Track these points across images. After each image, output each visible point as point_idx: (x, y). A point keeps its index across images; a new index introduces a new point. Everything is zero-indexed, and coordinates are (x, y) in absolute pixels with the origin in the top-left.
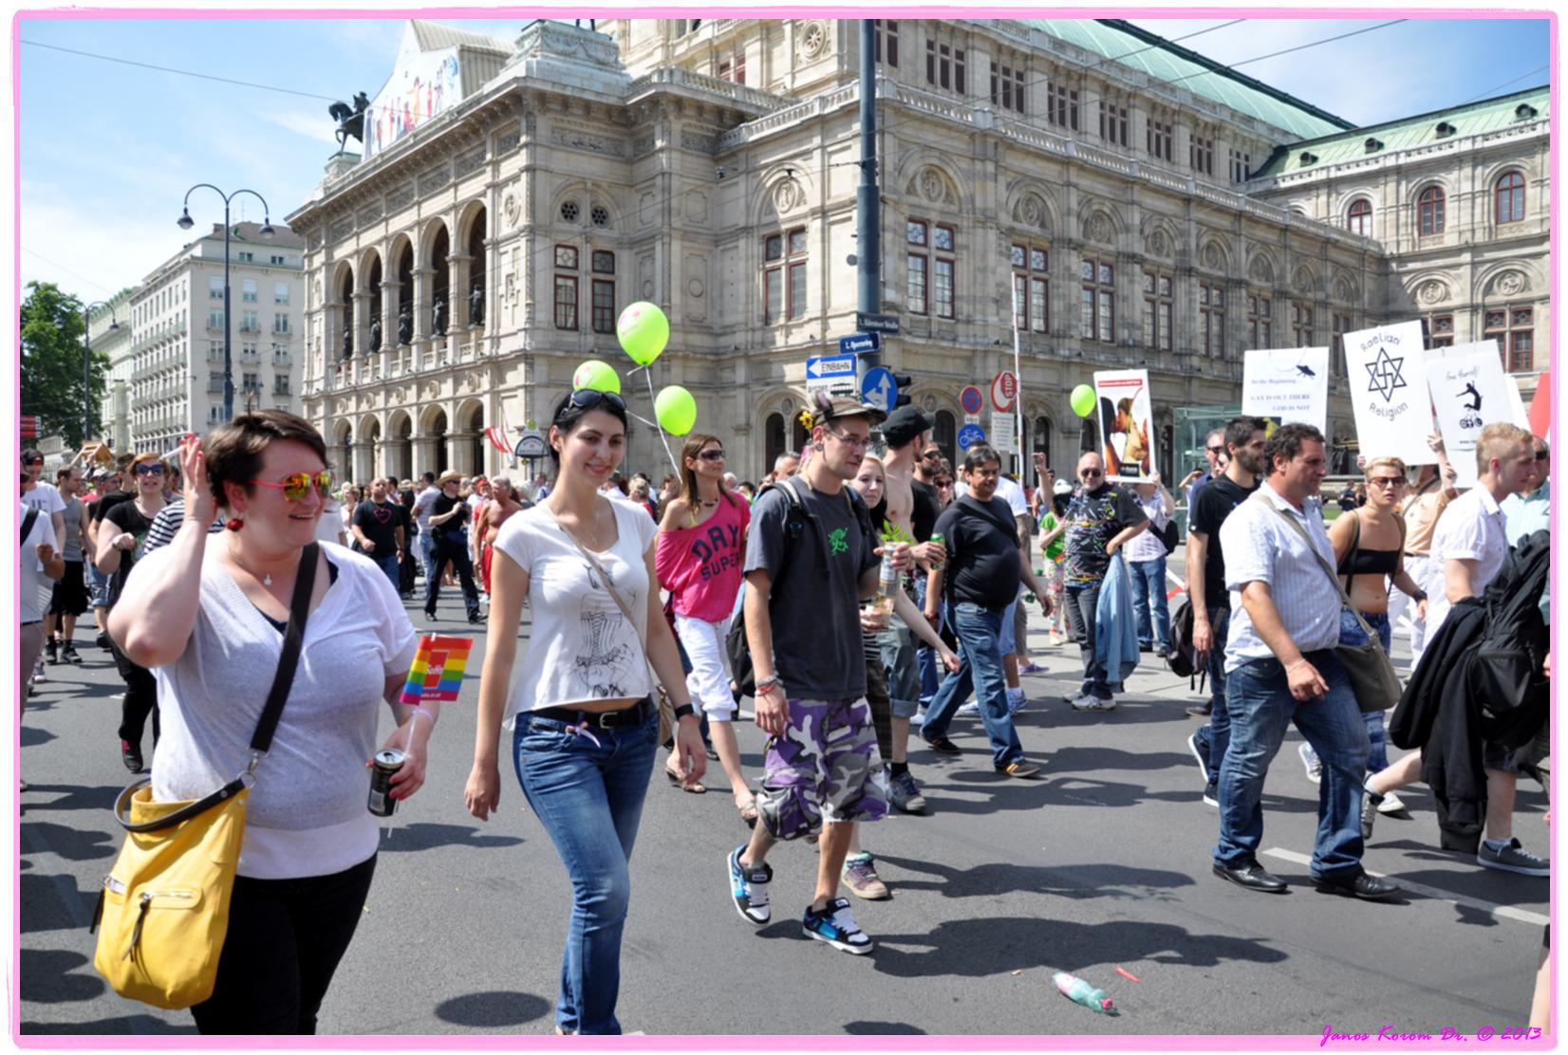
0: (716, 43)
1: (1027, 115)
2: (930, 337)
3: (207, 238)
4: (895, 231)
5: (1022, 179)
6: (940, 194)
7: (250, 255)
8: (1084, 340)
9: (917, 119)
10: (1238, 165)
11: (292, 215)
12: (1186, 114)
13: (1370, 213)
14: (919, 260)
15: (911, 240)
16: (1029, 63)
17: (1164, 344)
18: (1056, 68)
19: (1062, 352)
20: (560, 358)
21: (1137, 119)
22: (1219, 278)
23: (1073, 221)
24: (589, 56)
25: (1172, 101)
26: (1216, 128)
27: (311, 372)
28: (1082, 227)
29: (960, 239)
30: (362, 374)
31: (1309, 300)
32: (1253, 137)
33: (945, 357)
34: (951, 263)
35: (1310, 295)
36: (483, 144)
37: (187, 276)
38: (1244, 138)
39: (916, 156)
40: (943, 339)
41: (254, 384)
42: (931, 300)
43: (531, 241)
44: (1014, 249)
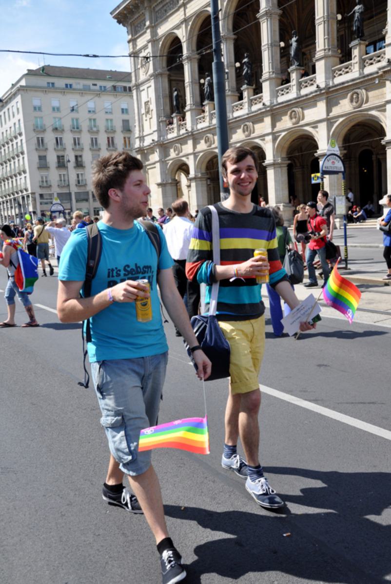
3: (27, 74)
7: (53, 84)
11: (118, 7)
27: (142, 128)
30: (195, 122)
37: (18, 98)
41: (63, 162)
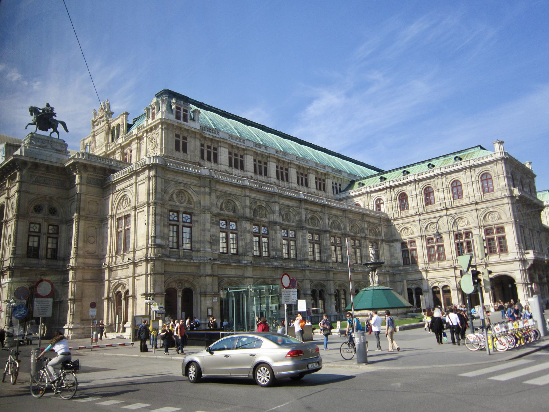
0: (122, 145)
1: (245, 171)
2: (179, 258)
4: (161, 216)
5: (225, 194)
6: (185, 201)
8: (254, 257)
9: (173, 171)
10: (336, 188)
12: (312, 170)
13: (383, 203)
14: (175, 228)
15: (171, 218)
16: (245, 152)
17: (293, 256)
18: (256, 154)
19: (244, 262)
20: (26, 270)
21: (292, 172)
22: (317, 230)
23: (248, 210)
24: (52, 148)
25: (307, 166)
26: (326, 174)
28: (252, 212)
29: (194, 218)
31: (358, 237)
32: (342, 177)
33: (187, 266)
34: (191, 228)
35: (359, 235)
38: (338, 178)
39: (174, 186)
40: (186, 259)
42: (181, 243)
43: (17, 221)
44: (221, 222)
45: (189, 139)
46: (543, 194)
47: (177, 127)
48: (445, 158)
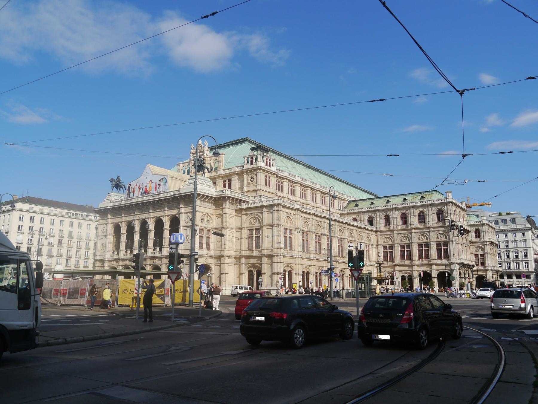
23: (313, 227)
29: (293, 232)
36: (180, 202)
45: (271, 178)
46: (470, 217)
47: (267, 171)
48: (414, 195)
